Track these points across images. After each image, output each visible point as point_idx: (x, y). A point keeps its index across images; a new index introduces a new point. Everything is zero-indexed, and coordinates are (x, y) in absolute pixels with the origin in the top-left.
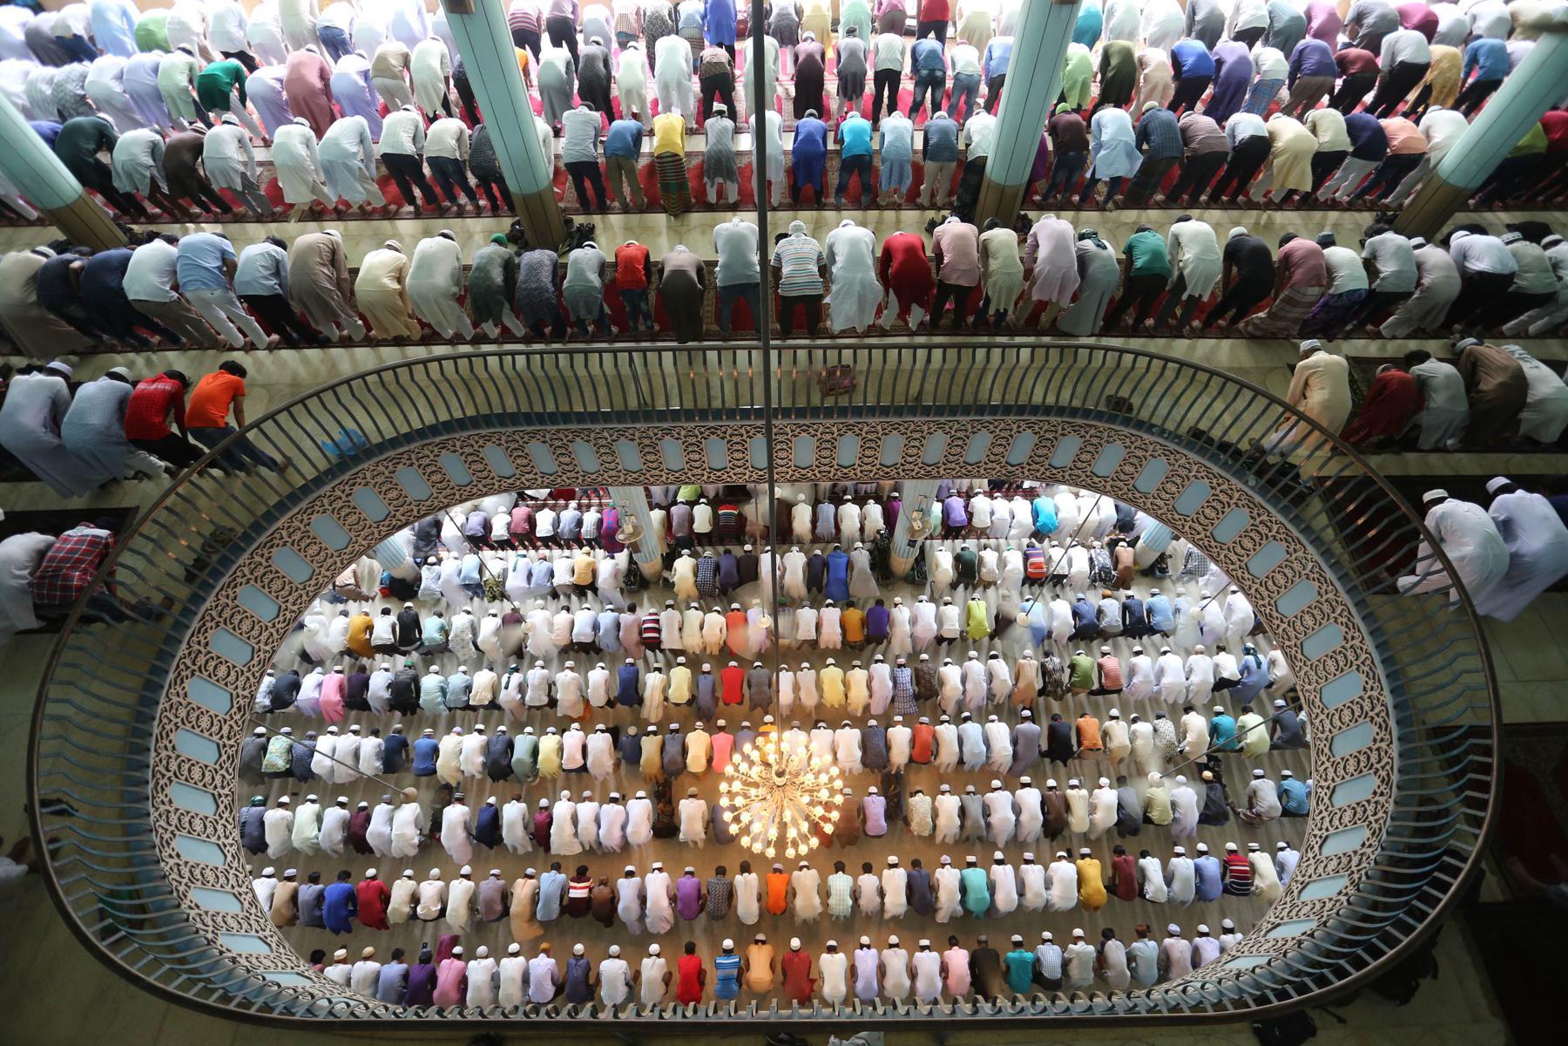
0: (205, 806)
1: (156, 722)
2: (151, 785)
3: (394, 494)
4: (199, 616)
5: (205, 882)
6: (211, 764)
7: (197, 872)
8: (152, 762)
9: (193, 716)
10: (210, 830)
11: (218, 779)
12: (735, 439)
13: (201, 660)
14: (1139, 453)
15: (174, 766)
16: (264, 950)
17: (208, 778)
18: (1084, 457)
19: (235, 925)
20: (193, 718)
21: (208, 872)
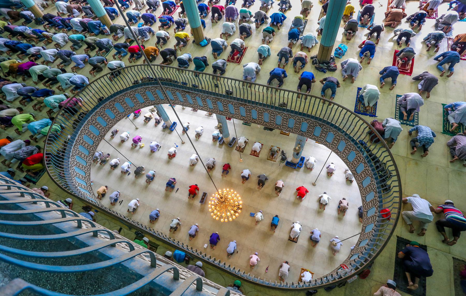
0: (86, 153)
1: (80, 131)
2: (74, 143)
3: (145, 97)
4: (95, 112)
5: (79, 166)
6: (91, 145)
7: (78, 164)
8: (76, 139)
9: (89, 133)
10: (85, 158)
11: (91, 149)
12: (224, 103)
13: (94, 122)
14: (338, 137)
15: (81, 142)
16: (85, 185)
17: (89, 147)
18: (323, 134)
19: (81, 177)
20: (89, 134)
21: (81, 165)
